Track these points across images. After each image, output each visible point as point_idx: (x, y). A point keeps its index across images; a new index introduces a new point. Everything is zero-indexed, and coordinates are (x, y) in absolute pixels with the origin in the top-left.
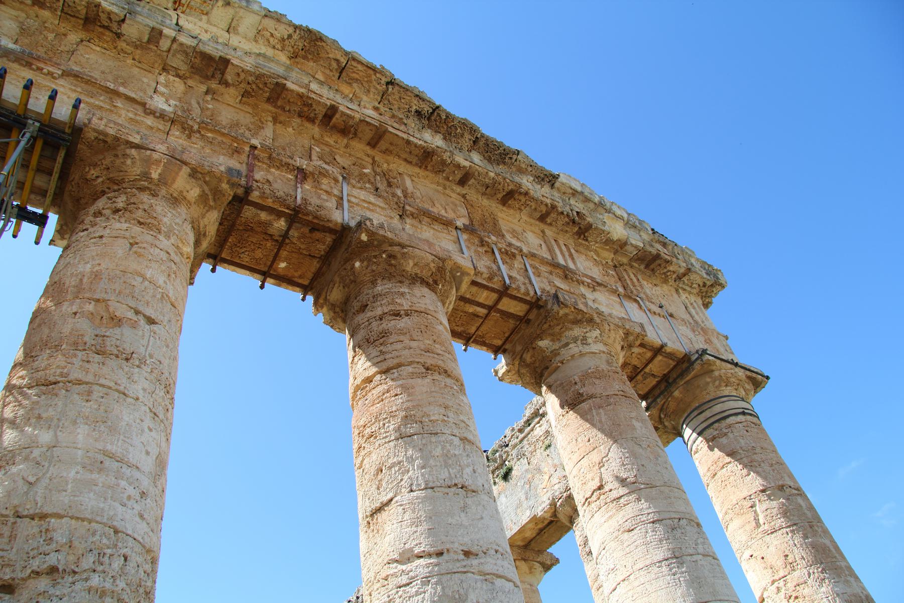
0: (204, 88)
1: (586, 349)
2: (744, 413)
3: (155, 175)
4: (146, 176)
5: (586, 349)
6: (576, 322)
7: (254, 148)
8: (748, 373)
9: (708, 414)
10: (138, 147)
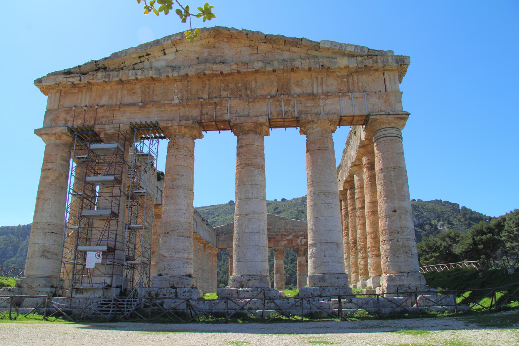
0: (186, 82)
1: (313, 131)
2: (386, 137)
3: (177, 131)
4: (175, 132)
5: (313, 131)
6: (309, 123)
7: (201, 102)
8: (396, 116)
9: (376, 136)
10: (172, 126)
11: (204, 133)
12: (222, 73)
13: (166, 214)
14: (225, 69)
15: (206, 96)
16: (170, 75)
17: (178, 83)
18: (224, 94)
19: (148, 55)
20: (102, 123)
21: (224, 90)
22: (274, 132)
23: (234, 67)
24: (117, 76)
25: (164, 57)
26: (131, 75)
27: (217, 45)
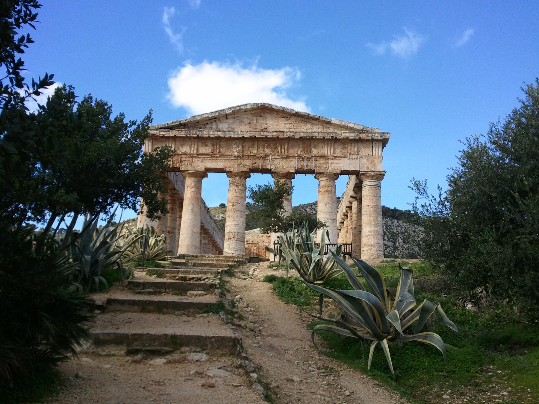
11: (251, 174)
12: (266, 137)
13: (229, 227)
14: (269, 135)
15: (255, 152)
16: (232, 136)
17: (237, 141)
18: (267, 151)
19: (215, 118)
20: (185, 164)
21: (267, 148)
22: (297, 176)
23: (275, 134)
24: (196, 134)
25: (227, 120)
26: (205, 134)
27: (262, 115)
